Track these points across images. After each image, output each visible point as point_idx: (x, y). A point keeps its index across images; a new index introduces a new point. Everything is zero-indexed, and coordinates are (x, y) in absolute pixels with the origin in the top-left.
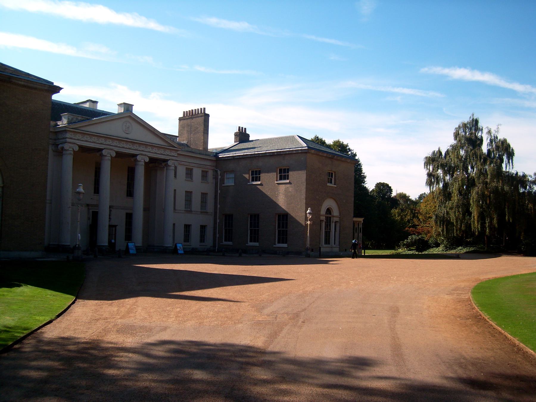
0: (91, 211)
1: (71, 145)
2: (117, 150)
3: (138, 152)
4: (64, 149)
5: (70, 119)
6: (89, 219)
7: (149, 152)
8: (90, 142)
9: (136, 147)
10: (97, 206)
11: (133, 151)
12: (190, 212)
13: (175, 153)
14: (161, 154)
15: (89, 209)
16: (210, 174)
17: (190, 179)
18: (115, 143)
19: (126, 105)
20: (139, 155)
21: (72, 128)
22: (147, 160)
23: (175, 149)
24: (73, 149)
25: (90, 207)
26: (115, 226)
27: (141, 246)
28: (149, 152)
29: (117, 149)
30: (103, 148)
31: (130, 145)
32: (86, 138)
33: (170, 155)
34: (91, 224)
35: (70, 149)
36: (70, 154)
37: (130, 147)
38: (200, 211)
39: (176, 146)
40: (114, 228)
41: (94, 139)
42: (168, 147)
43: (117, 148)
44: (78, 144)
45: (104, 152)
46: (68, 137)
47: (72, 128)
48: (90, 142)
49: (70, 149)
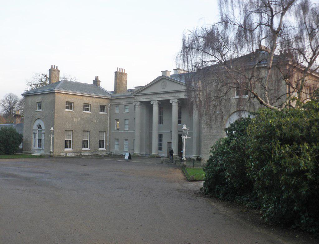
18: (158, 96)
21: (136, 94)
47: (136, 94)
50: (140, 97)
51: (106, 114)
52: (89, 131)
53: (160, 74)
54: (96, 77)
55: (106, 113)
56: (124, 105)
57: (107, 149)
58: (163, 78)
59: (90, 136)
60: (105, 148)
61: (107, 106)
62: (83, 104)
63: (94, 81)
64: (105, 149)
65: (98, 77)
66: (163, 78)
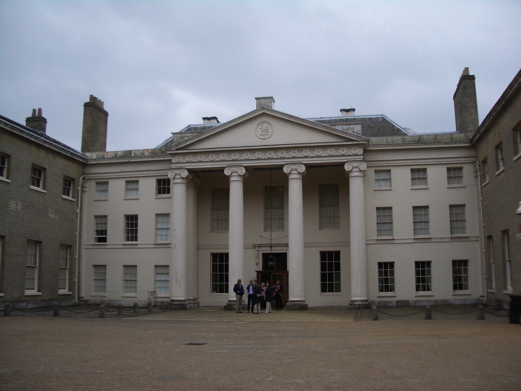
6: (257, 264)
7: (306, 157)
8: (195, 162)
12: (428, 240)
13: (358, 149)
14: (331, 156)
16: (468, 171)
17: (424, 187)
18: (245, 156)
20: (285, 165)
23: (358, 143)
27: (304, 301)
28: (306, 157)
32: (198, 158)
33: (348, 154)
37: (270, 156)
38: (450, 236)
39: (355, 139)
41: (214, 157)
42: (341, 143)
43: (248, 162)
44: (186, 168)
46: (175, 162)
50: (188, 159)
51: (74, 200)
52: (40, 242)
53: (251, 107)
54: (34, 110)
55: (73, 198)
56: (122, 183)
57: (74, 293)
58: (264, 114)
59: (40, 257)
60: (70, 291)
61: (76, 181)
62: (30, 167)
63: (28, 120)
64: (71, 293)
65: (40, 110)
66: (264, 114)
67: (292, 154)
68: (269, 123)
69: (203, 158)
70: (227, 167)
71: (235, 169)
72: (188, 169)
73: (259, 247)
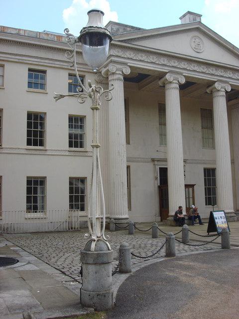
0: (158, 167)
1: (119, 66)
2: (186, 75)
3: (215, 77)
4: (109, 74)
5: (115, 29)
6: (156, 178)
9: (212, 70)
10: (165, 160)
11: (208, 76)
15: (154, 165)
18: (183, 65)
19: (192, 16)
20: (216, 81)
21: (119, 41)
22: (229, 89)
24: (123, 73)
25: (156, 163)
26: (192, 186)
29: (186, 73)
30: (167, 71)
31: (204, 69)
32: (140, 56)
34: (159, 185)
35: (118, 72)
36: (119, 79)
37: (204, 71)
40: (191, 189)
41: (152, 58)
43: (186, 72)
45: (168, 77)
47: (119, 41)
48: (148, 62)
49: (118, 72)
50: (129, 54)
58: (198, 29)
66: (198, 29)
67: (219, 72)
68: (201, 39)
69: (144, 57)
70: (169, 72)
71: (177, 76)
72: (134, 67)
73: (158, 161)
